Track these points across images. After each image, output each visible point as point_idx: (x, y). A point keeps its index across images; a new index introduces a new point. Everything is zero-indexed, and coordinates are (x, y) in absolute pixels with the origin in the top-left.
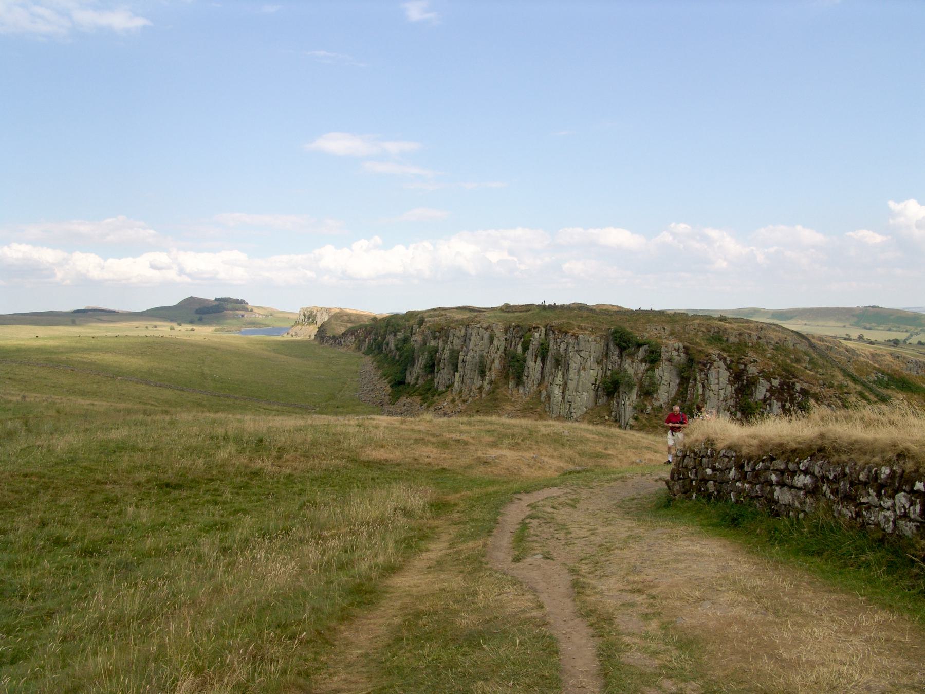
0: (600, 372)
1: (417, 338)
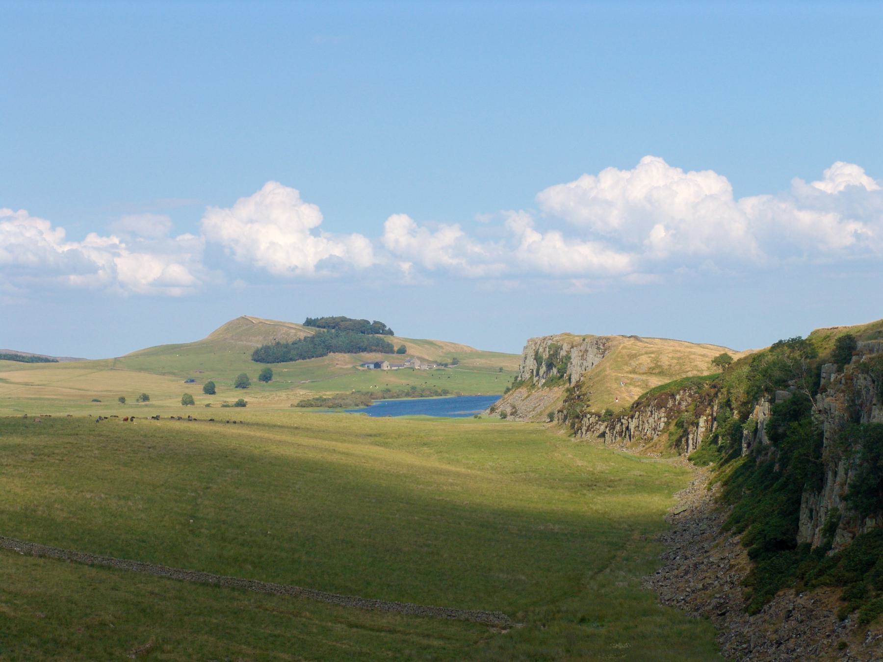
1: (830, 405)
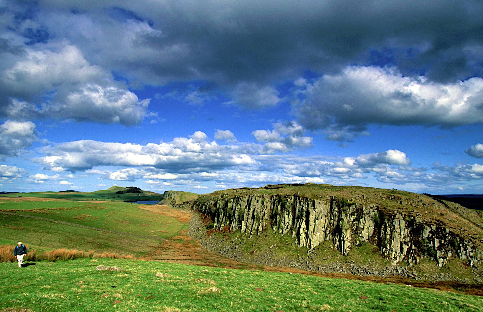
0: (327, 220)
